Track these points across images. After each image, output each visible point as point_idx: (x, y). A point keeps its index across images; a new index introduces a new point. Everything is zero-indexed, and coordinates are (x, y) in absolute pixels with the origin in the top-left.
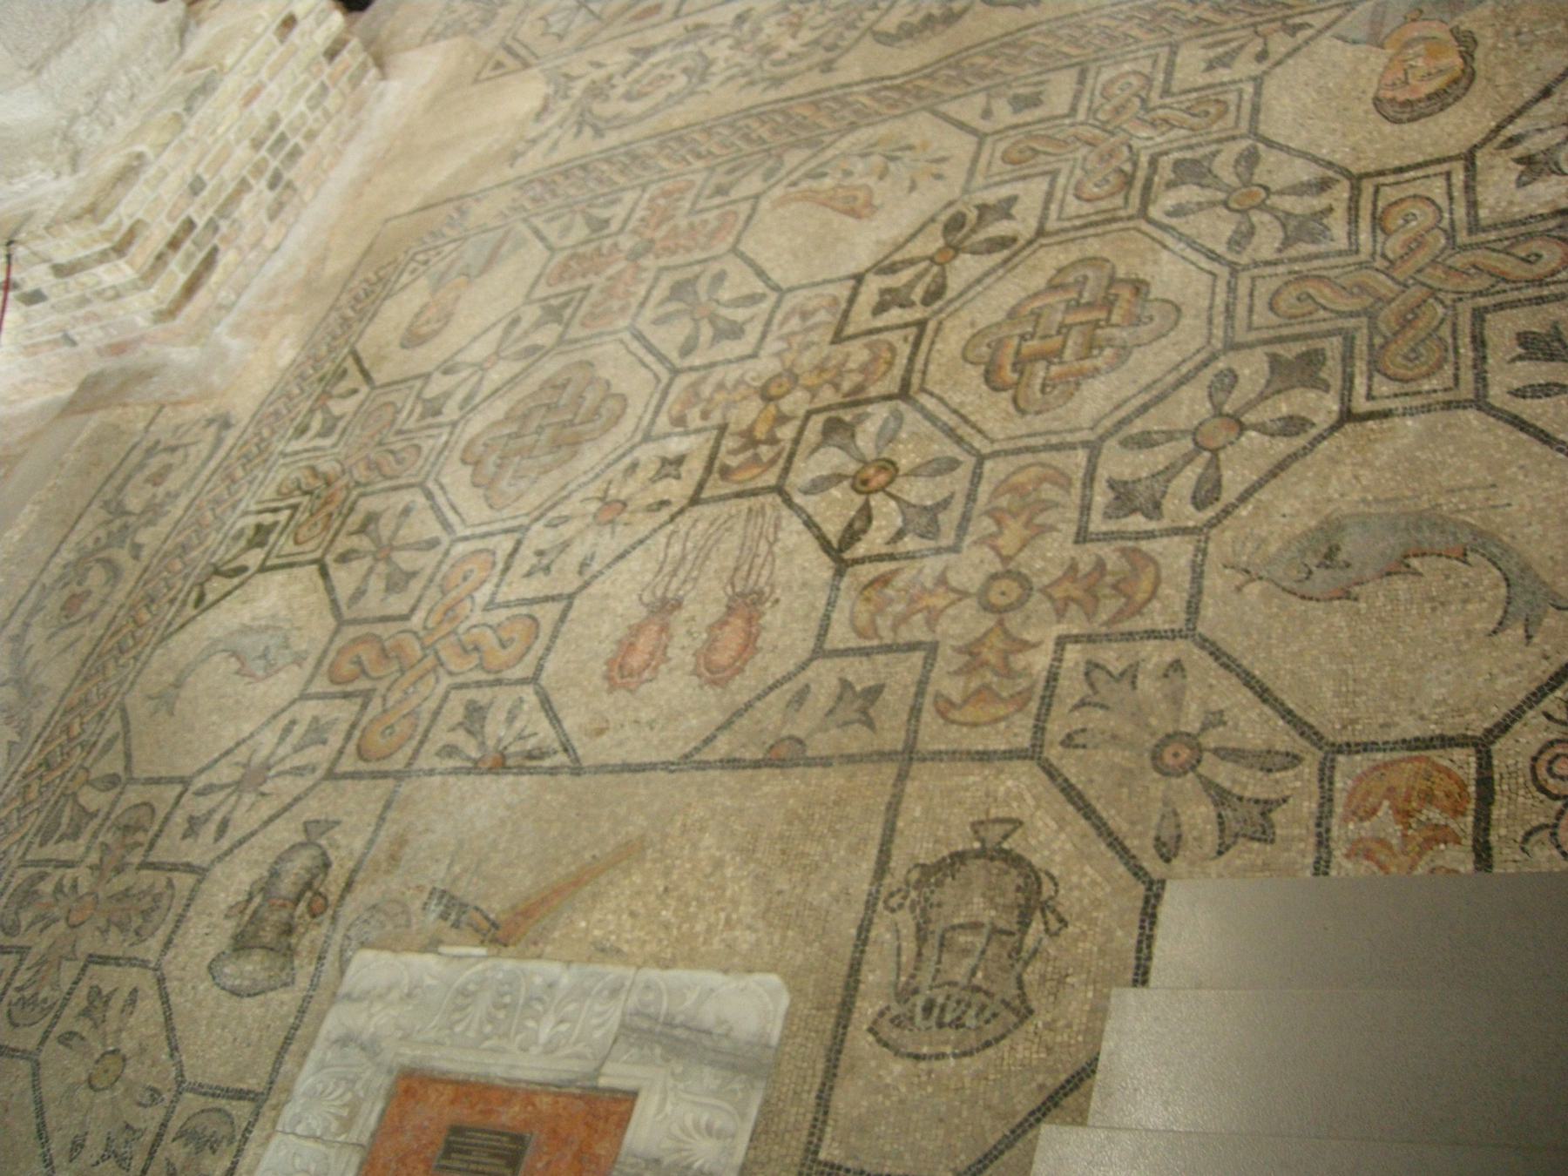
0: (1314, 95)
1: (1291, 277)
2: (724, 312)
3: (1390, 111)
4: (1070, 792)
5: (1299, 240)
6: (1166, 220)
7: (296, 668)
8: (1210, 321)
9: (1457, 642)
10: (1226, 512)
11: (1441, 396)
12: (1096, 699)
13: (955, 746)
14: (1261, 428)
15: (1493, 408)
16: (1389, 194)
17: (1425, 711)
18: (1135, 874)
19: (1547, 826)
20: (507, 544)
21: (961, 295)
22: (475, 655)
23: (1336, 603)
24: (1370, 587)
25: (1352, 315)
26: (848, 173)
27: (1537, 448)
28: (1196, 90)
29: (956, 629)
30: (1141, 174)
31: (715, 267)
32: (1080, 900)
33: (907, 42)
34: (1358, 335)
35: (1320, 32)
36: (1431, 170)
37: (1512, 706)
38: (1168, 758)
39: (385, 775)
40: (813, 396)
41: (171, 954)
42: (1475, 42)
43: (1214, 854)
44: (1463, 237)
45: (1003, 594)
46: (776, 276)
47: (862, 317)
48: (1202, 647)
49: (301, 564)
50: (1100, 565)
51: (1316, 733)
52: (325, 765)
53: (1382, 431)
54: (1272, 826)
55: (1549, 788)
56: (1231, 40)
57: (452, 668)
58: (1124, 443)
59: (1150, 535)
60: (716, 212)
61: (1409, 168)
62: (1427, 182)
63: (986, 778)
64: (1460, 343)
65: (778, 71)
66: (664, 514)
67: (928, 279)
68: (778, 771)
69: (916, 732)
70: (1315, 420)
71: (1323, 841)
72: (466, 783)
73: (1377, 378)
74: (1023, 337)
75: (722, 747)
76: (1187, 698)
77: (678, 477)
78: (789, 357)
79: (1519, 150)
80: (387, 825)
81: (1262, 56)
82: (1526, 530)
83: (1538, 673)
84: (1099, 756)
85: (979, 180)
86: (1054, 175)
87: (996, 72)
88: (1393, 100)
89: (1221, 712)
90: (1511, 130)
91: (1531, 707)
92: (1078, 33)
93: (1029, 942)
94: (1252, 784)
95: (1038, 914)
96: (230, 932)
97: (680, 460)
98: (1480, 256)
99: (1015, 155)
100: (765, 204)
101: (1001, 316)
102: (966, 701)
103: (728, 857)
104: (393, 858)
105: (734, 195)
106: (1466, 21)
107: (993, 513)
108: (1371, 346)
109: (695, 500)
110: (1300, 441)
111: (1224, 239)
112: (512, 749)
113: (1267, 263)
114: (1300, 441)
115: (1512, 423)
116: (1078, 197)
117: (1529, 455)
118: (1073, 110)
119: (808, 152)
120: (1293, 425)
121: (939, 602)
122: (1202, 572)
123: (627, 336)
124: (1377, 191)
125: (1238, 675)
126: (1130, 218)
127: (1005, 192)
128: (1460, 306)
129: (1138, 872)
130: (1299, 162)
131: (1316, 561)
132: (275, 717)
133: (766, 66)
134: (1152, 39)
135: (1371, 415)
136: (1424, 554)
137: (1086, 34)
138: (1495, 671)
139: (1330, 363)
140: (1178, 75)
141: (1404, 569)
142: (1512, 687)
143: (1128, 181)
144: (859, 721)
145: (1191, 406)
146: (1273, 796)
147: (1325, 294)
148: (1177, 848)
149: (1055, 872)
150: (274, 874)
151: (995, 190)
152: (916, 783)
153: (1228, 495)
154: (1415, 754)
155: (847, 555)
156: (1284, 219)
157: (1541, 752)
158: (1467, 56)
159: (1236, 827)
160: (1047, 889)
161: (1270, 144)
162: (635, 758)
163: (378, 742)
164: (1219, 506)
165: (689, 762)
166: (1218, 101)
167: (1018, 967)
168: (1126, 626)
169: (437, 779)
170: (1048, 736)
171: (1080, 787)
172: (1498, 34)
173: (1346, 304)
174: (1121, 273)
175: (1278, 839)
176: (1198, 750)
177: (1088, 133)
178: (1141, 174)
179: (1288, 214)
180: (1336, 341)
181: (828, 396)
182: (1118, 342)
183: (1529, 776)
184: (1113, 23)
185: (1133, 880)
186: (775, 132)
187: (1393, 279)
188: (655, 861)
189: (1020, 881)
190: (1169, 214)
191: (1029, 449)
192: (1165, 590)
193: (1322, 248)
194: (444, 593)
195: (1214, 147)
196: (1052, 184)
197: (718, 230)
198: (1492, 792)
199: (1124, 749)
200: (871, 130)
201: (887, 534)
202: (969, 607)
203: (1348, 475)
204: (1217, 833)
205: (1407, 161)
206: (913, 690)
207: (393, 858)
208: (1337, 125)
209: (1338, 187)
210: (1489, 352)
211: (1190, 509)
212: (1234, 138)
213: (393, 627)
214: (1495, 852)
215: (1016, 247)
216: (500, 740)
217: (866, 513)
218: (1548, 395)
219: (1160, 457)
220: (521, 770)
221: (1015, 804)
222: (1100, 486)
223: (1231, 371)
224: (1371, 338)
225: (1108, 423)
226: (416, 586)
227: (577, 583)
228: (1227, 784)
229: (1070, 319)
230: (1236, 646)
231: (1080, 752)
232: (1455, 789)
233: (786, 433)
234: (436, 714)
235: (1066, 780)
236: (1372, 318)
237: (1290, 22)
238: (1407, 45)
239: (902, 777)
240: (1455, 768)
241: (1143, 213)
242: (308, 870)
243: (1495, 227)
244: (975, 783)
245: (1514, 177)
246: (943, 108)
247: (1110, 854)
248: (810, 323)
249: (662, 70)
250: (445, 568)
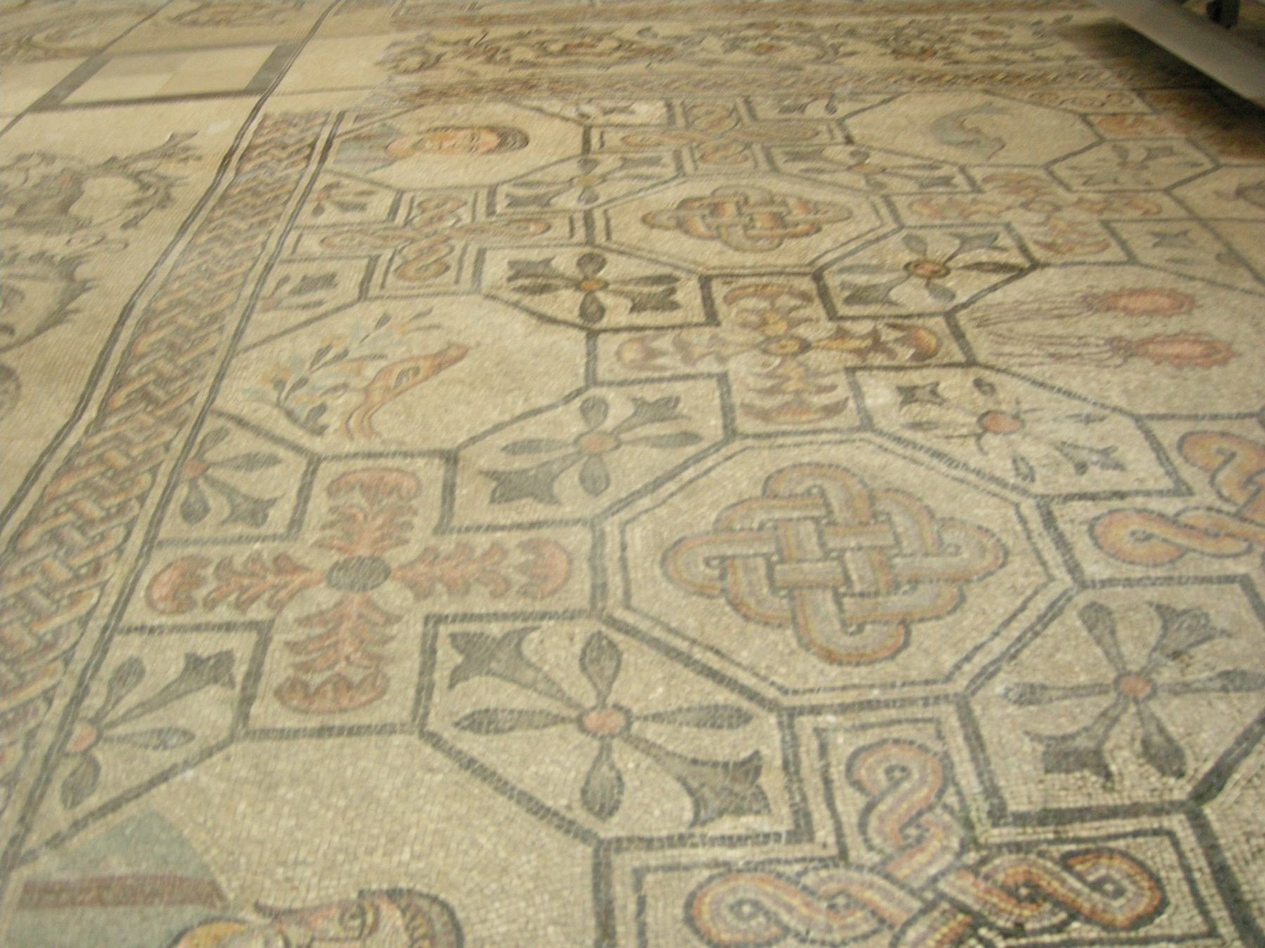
49: (1211, 847)
194: (1183, 552)
226: (1185, 597)
227: (1117, 417)
250: (1138, 572)
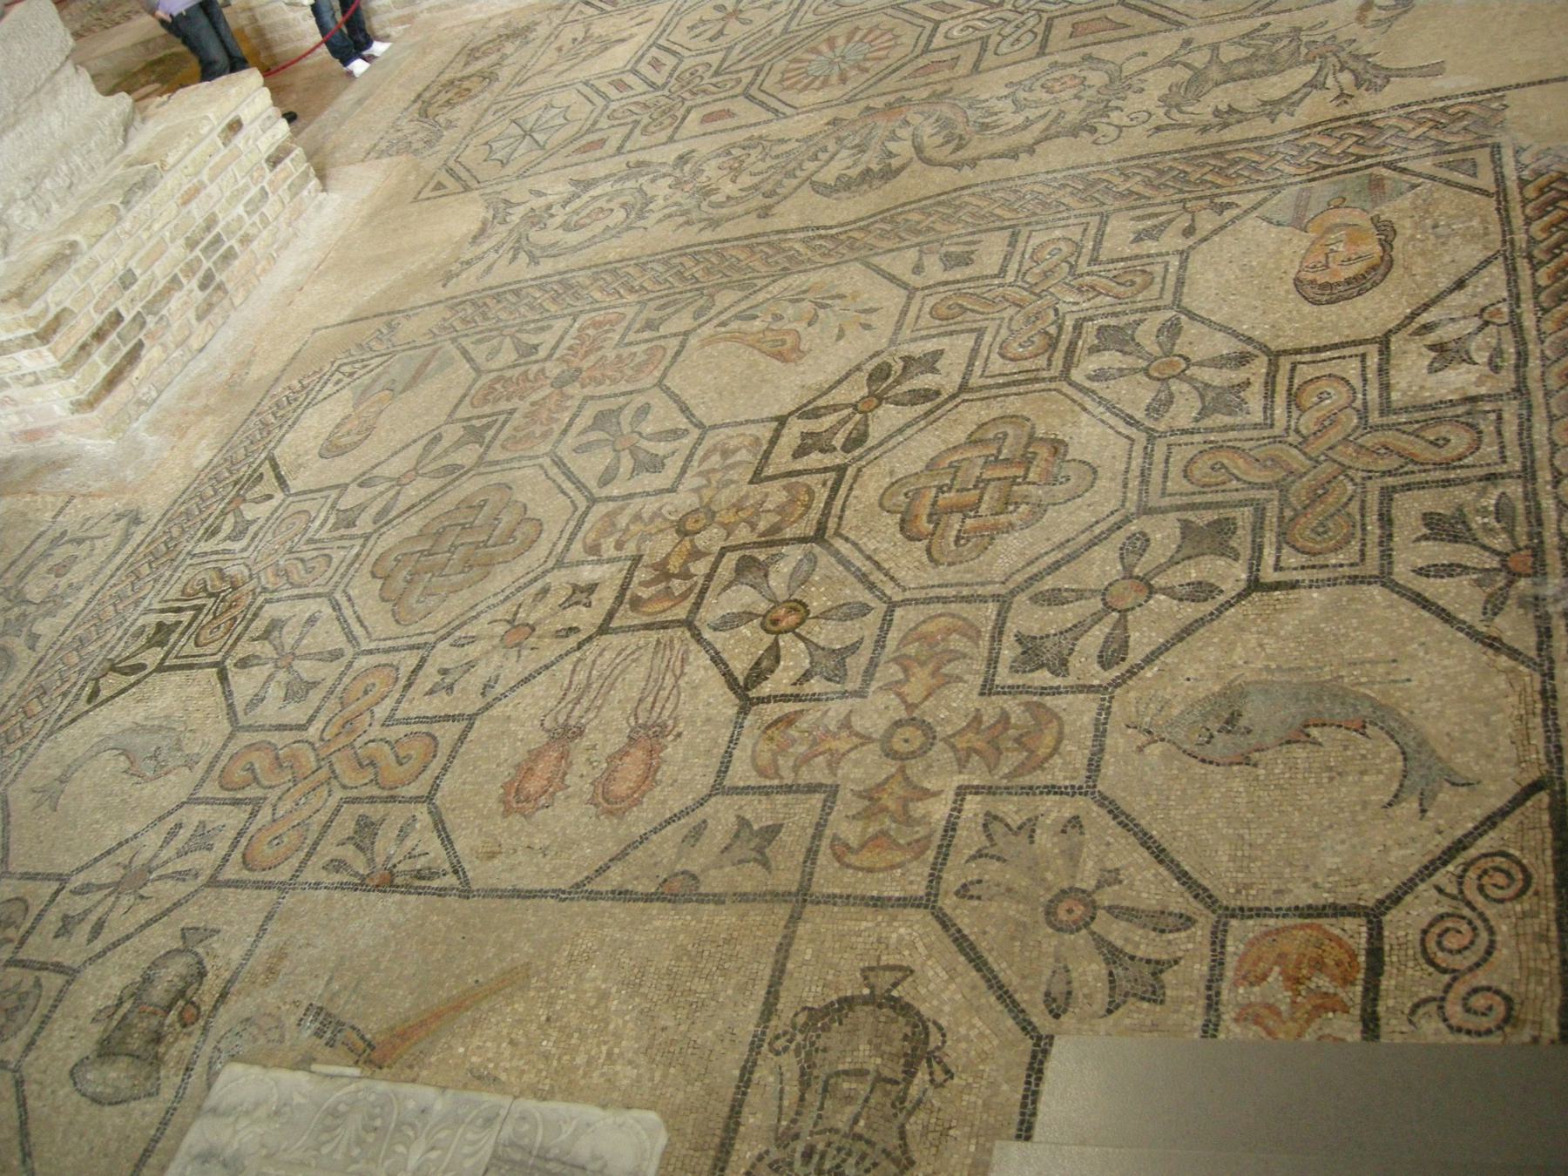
0: (1238, 272)
1: (1207, 446)
2: (644, 444)
3: (1309, 292)
4: (962, 942)
5: (1215, 411)
6: (1087, 384)
7: (187, 771)
8: (1125, 486)
9: (1353, 813)
10: (1131, 673)
11: (1347, 571)
12: (992, 851)
13: (850, 891)
14: (1169, 592)
15: (1397, 584)
16: (1306, 372)
17: (1319, 880)
18: (1024, 1029)
19: (1434, 999)
20: (412, 660)
21: (881, 444)
22: (371, 769)
23: (1235, 768)
24: (1270, 754)
25: (1263, 486)
26: (778, 318)
27: (1438, 626)
28: (1122, 260)
29: (858, 773)
30: (1065, 338)
31: (640, 400)
32: (967, 1052)
33: (843, 195)
34: (1269, 507)
35: (1246, 212)
36: (1346, 352)
37: (1405, 878)
38: (1062, 915)
39: (268, 886)
40: (728, 535)
41: (32, 1056)
42: (1395, 232)
43: (1103, 1012)
44: (1374, 418)
45: (906, 741)
46: (699, 413)
47: (782, 459)
48: (1101, 805)
49: (201, 666)
50: (1005, 718)
51: (1210, 896)
52: (209, 872)
53: (1288, 601)
54: (1163, 987)
55: (1438, 961)
56: (1161, 214)
57: (346, 781)
58: (1034, 599)
59: (1056, 691)
60: (644, 346)
61: (1326, 348)
62: (1343, 362)
63: (878, 924)
64: (1368, 520)
65: (715, 213)
66: (572, 641)
67: (850, 426)
68: (669, 906)
69: (811, 874)
70: (1223, 587)
71: (1212, 1004)
72: (352, 898)
73: (1286, 550)
74: (940, 489)
75: (615, 877)
76: (1084, 855)
77: (588, 605)
78: (707, 493)
79: (1432, 338)
80: (267, 937)
81: (1189, 232)
82: (1425, 706)
83: (1430, 847)
84: (993, 908)
85: (906, 333)
86: (981, 332)
87: (929, 229)
88: (1313, 282)
89: (1117, 870)
90: (1426, 318)
91: (1423, 880)
92: (1012, 197)
93: (914, 1092)
94: (1145, 944)
95: (924, 1063)
96: (97, 1037)
97: (592, 588)
98: (1390, 437)
99: (943, 311)
100: (693, 341)
101: (920, 466)
102: (863, 846)
103: (614, 990)
104: (271, 971)
105: (663, 331)
106: (1387, 211)
107: (901, 661)
108: (1281, 518)
109: (603, 629)
110: (1208, 607)
111: (1144, 406)
112: (401, 867)
113: (1184, 432)
114: (1208, 607)
115: (1414, 600)
116: (1003, 356)
117: (1430, 632)
118: (1003, 271)
119: (741, 294)
120: (1202, 591)
121: (843, 746)
122: (1105, 731)
123: (547, 462)
124: (1293, 370)
125: (1135, 834)
126: (1052, 379)
127: (931, 346)
128: (1369, 484)
129: (1027, 1027)
130: (1219, 335)
131: (1217, 726)
132: (161, 819)
133: (704, 205)
134: (1083, 208)
135: (1277, 586)
136: (1324, 725)
137: (1019, 199)
138: (1389, 843)
139: (1240, 532)
140: (1106, 244)
141: (1303, 738)
142: (1409, 859)
143: (1053, 344)
144: (755, 860)
145: (1102, 566)
146: (1165, 957)
147: (1239, 465)
148: (1067, 1004)
149: (943, 1022)
150: (147, 980)
151: (921, 343)
152: (809, 926)
153: (1134, 657)
154: (1308, 921)
155: (753, 694)
156: (1203, 389)
157: (1431, 925)
158: (1387, 245)
159: (1126, 986)
160: (935, 1040)
161: (1192, 316)
162: (525, 885)
163: (265, 851)
164: (1125, 666)
165: (580, 891)
166: (1144, 272)
167: (901, 1117)
168: (1027, 780)
169: (322, 893)
170: (943, 886)
171: (972, 938)
172: (1416, 225)
173: (1257, 476)
174: (1040, 433)
175: (1168, 999)
176: (1094, 906)
177: (1014, 293)
178: (1065, 338)
179: (1207, 385)
180: (1247, 511)
181: (743, 534)
182: (1033, 500)
183: (1419, 949)
184: (1047, 190)
185: (1021, 1034)
186: (708, 272)
187: (1305, 454)
188: (539, 990)
189: (908, 1030)
190: (1090, 378)
191: (938, 599)
192: (1067, 746)
193: (1238, 420)
194: (343, 705)
195: (1138, 316)
196: (978, 341)
197: (646, 363)
198: (1382, 963)
199: (1019, 902)
200: (803, 277)
201: (794, 674)
202: (872, 753)
203: (1253, 643)
204: (1107, 991)
205: (1324, 342)
206: (810, 831)
207: (271, 971)
208: (1258, 303)
209: (1257, 361)
210: (1395, 530)
211: (1097, 667)
212: (1158, 308)
213: (289, 736)
214: (1382, 1022)
215: (939, 400)
216: (389, 858)
217: (774, 653)
218: (1451, 576)
219: (1069, 615)
220: (408, 889)
221: (906, 953)
222: (1009, 639)
223: (1144, 534)
224: (1281, 511)
225: (1019, 578)
226: (315, 697)
227: (480, 704)
228: (1119, 943)
229: (986, 475)
230: (1136, 805)
231: (975, 903)
232: (1345, 958)
233: (700, 568)
234: (326, 826)
235: (959, 931)
236: (1283, 491)
237: (1217, 200)
238: (1329, 230)
239: (795, 918)
240: (1345, 938)
241: (1065, 375)
242: (183, 978)
243: (1406, 410)
244: (867, 929)
245: (1427, 363)
246: (875, 260)
247: (1000, 1007)
248: (729, 461)
249: (602, 203)
250: (346, 680)
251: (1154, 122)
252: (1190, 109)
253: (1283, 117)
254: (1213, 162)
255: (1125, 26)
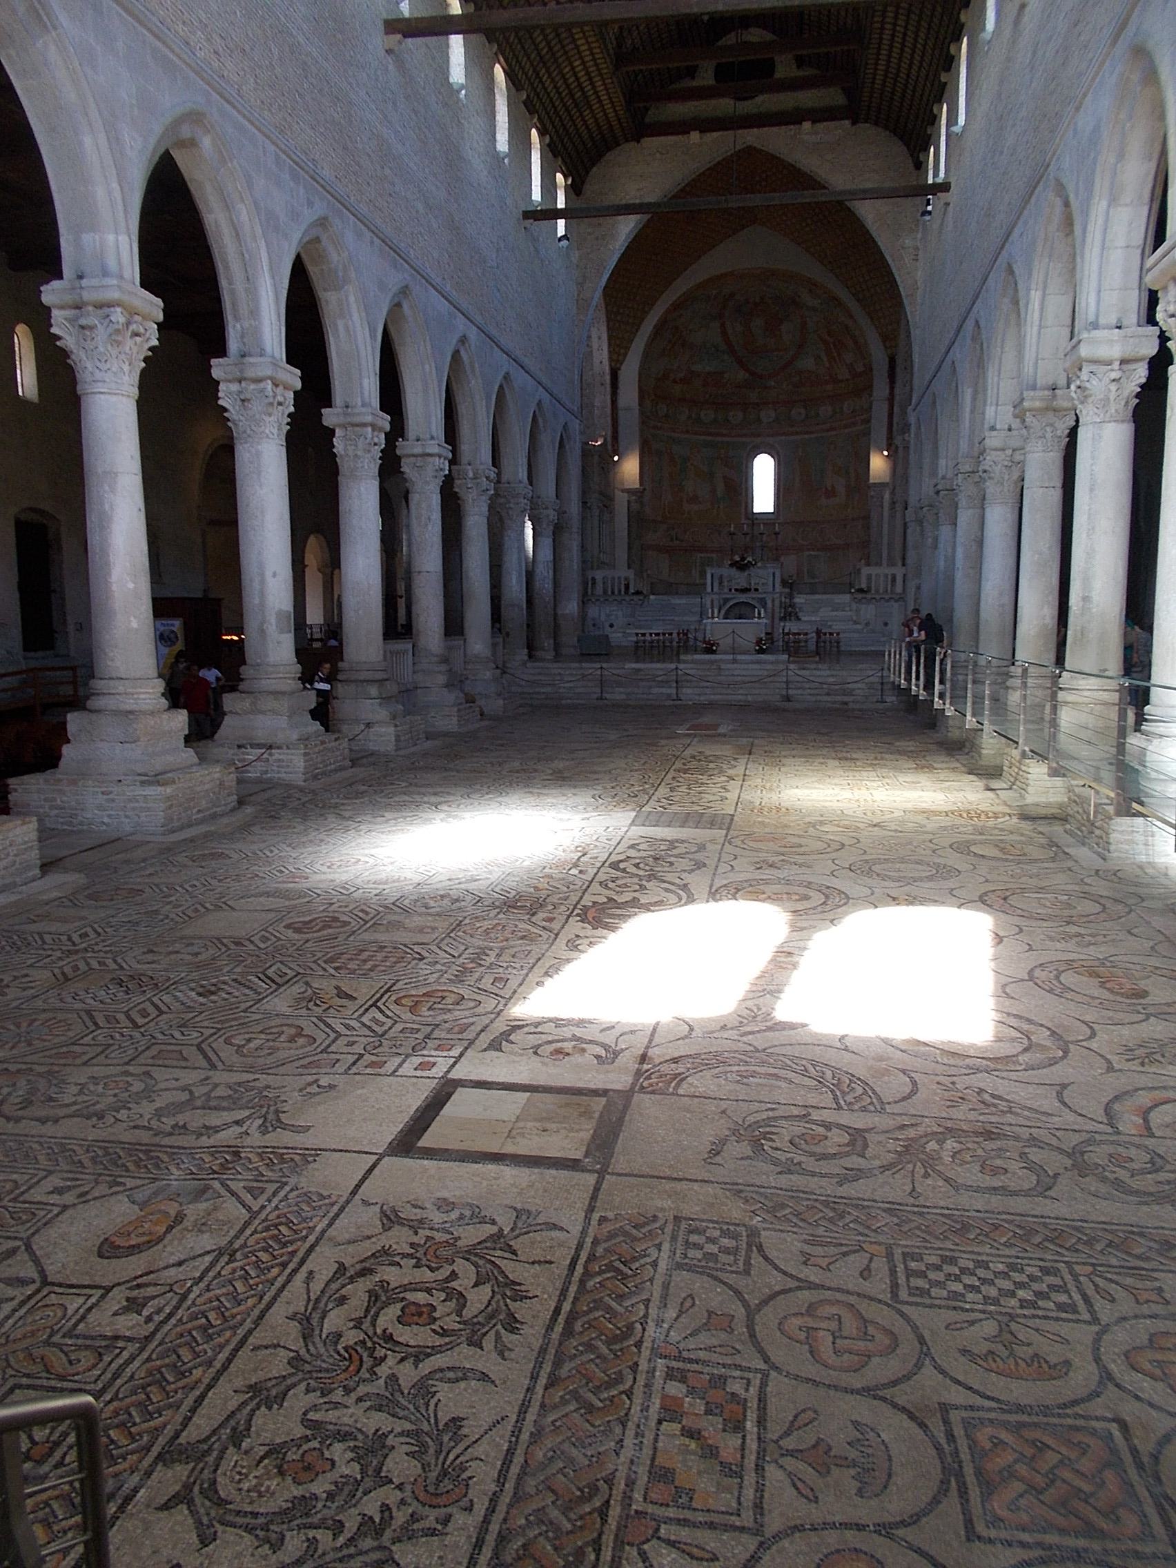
251: (139, 1123)
252: (164, 1120)
253: (204, 1138)
254: (141, 1155)
255: (186, 1059)
